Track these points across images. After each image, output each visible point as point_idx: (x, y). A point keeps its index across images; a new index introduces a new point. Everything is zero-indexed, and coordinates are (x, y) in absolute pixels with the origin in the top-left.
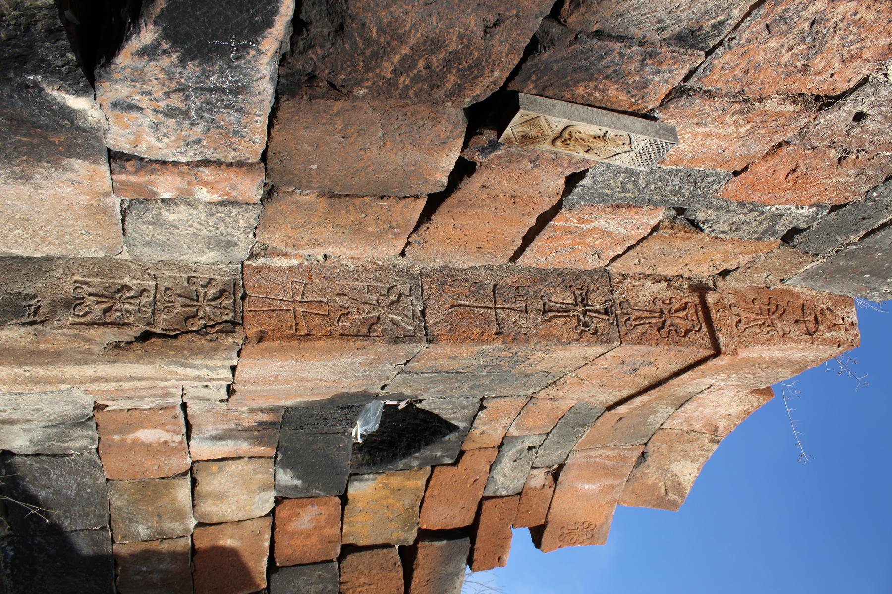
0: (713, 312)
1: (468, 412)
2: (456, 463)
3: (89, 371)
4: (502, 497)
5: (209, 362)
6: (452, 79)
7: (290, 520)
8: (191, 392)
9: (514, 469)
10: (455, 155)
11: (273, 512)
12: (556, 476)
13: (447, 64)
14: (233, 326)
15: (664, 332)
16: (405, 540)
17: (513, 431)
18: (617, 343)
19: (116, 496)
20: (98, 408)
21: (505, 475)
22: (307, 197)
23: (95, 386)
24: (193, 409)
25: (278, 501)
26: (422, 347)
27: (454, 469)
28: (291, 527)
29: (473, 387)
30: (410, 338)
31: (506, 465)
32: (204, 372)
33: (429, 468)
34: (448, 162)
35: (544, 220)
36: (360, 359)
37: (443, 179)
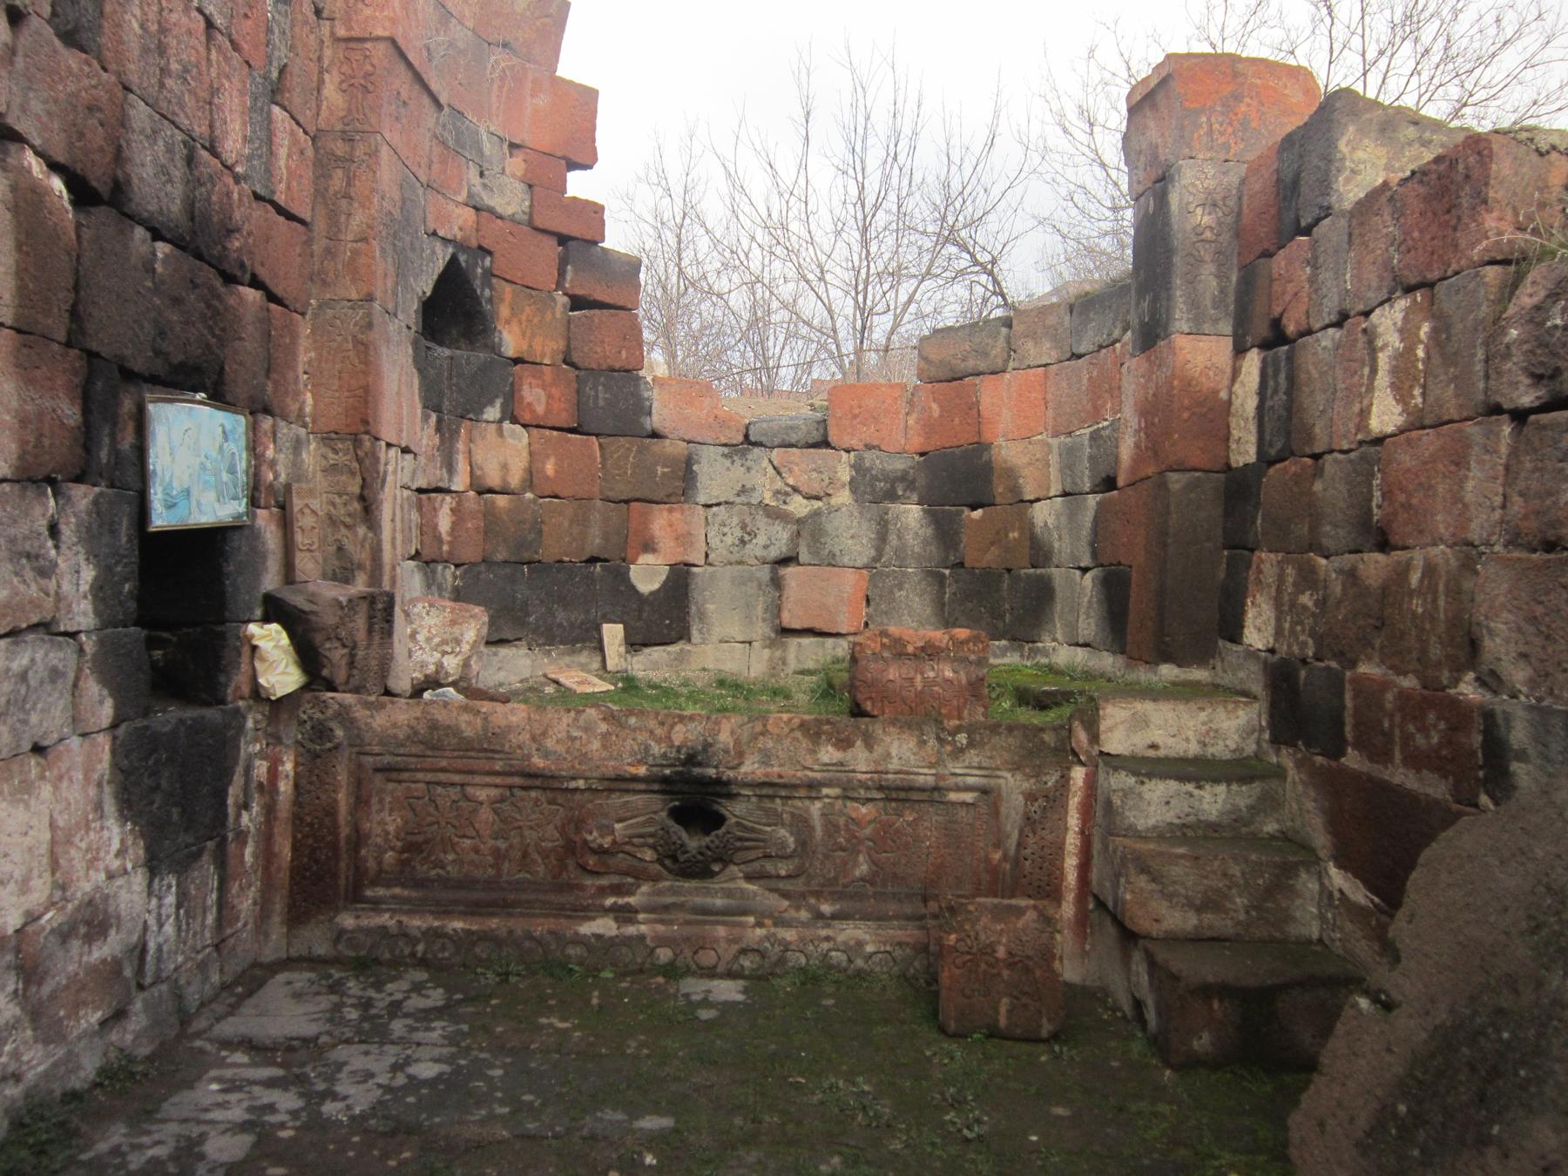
0: (353, 34)
1: (438, 246)
2: (490, 253)
4: (531, 206)
5: (382, 461)
6: (215, 303)
7: (533, 411)
8: (406, 480)
9: (502, 193)
11: (525, 426)
12: (513, 146)
13: (209, 306)
14: (357, 442)
15: (371, 88)
16: (564, 306)
17: (461, 198)
18: (379, 137)
20: (416, 556)
21: (508, 204)
22: (270, 387)
23: (399, 551)
24: (422, 483)
25: (514, 421)
26: (376, 305)
27: (497, 255)
28: (540, 409)
29: (413, 249)
30: (369, 315)
32: (390, 468)
33: (494, 280)
34: (251, 295)
35: (281, 211)
36: (384, 350)
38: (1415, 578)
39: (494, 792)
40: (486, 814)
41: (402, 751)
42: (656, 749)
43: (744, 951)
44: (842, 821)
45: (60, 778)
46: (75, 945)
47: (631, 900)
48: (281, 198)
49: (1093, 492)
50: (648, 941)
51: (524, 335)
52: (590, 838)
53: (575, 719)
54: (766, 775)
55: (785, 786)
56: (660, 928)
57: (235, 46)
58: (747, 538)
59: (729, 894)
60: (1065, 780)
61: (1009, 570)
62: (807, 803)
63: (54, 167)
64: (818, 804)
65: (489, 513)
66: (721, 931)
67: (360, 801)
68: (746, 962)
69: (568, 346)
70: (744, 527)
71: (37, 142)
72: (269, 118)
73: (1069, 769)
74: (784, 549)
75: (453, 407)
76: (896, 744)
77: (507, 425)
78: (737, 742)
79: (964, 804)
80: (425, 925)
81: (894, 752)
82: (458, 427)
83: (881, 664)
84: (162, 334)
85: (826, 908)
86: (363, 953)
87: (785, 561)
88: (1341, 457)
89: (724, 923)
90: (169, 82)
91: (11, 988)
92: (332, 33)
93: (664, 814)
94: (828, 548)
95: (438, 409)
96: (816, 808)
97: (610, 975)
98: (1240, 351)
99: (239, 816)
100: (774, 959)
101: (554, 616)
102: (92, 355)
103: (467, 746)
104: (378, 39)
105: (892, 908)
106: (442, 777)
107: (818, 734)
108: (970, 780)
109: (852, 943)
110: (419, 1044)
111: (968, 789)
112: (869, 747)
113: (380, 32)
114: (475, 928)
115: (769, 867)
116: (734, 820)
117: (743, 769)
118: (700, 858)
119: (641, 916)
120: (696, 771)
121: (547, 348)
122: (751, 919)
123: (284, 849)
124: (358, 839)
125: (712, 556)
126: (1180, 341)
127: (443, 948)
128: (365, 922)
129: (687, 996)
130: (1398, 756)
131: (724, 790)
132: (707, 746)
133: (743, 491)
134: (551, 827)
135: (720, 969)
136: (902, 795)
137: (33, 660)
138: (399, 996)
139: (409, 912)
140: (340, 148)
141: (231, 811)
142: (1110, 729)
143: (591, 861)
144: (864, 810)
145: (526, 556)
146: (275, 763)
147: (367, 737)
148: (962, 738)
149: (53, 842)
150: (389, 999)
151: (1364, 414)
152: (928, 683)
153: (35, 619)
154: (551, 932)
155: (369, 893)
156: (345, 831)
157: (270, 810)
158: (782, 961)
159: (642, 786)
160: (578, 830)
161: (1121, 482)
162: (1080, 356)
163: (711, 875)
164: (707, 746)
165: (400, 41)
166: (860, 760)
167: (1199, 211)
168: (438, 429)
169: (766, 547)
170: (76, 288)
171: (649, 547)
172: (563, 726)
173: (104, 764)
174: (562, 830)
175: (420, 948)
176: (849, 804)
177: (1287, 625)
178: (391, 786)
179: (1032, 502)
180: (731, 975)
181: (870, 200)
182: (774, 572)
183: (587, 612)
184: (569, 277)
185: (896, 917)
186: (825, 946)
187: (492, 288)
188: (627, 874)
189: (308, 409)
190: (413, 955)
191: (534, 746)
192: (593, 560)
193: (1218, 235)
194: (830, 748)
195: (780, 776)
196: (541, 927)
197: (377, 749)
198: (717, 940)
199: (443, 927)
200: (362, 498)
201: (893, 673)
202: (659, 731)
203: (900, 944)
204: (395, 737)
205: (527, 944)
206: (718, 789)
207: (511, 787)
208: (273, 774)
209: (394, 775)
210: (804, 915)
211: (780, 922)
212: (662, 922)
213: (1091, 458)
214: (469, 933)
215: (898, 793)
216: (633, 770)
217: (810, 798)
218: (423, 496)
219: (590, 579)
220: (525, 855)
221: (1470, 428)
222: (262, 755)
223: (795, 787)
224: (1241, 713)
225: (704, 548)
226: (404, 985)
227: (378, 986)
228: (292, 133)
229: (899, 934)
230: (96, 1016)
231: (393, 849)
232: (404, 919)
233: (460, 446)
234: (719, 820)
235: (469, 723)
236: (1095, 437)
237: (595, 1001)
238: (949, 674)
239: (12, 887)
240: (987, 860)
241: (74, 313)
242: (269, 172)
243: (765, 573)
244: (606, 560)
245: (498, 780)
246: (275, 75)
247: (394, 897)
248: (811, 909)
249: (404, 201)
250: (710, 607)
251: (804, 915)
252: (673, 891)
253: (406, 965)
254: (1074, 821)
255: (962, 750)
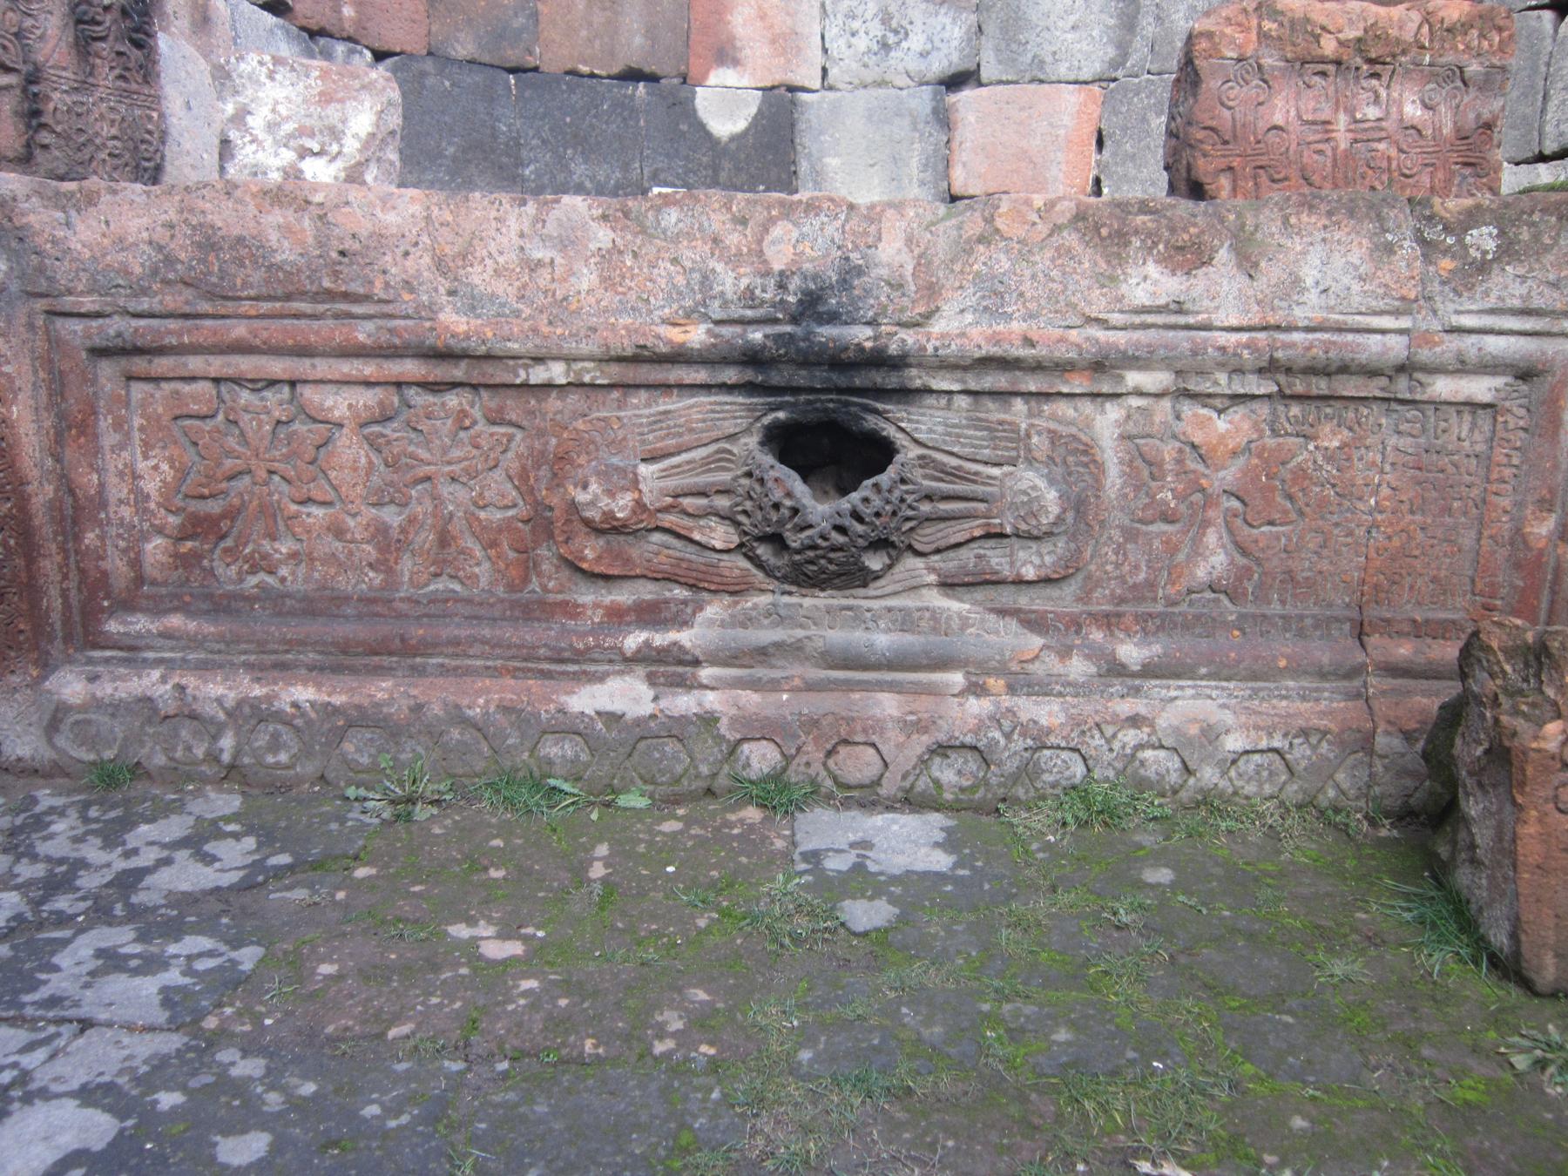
19: (459, 48)
40: (350, 449)
41: (145, 304)
42: (729, 281)
43: (942, 750)
44: (1168, 451)
47: (685, 637)
50: (723, 727)
52: (582, 497)
53: (539, 220)
54: (996, 339)
55: (1037, 367)
56: (751, 699)
58: (892, 39)
59: (906, 622)
62: (1087, 407)
64: (1114, 412)
66: (888, 705)
67: (73, 427)
68: (948, 774)
70: (886, 19)
74: (955, 58)
76: (1315, 258)
78: (923, 263)
80: (231, 697)
81: (1309, 275)
83: (1254, 88)
85: (1131, 652)
86: (109, 754)
87: (956, 81)
89: (892, 687)
93: (753, 441)
94: (1032, 49)
96: (1107, 423)
97: (642, 803)
100: (1011, 766)
101: (565, 168)
103: (287, 290)
105: (1283, 649)
106: (245, 365)
107: (1121, 237)
108: (1495, 345)
109: (1194, 730)
110: (86, 1025)
111: (1488, 367)
112: (1248, 264)
114: (339, 700)
115: (997, 559)
116: (915, 452)
117: (938, 327)
118: (839, 539)
119: (706, 673)
120: (826, 332)
122: (957, 678)
124: (77, 511)
125: (834, 72)
127: (275, 745)
128: (105, 689)
129: (814, 857)
131: (892, 381)
132: (850, 273)
134: (498, 474)
135: (888, 789)
136: (1321, 386)
138: (148, 857)
139: (203, 667)
143: (590, 550)
144: (1222, 425)
145: (513, 56)
147: (63, 273)
148: (1483, 239)
150: (121, 865)
152: (1364, 134)
154: (505, 709)
155: (113, 627)
156: (42, 493)
158: (1028, 771)
159: (701, 375)
160: (557, 480)
163: (864, 578)
164: (850, 273)
166: (1224, 297)
169: (924, 55)
171: (726, 55)
172: (510, 236)
174: (522, 479)
175: (227, 743)
176: (1188, 409)
178: (138, 390)
180: (911, 802)
182: (936, 97)
183: (626, 167)
185: (1295, 671)
186: (1130, 737)
188: (670, 579)
190: (213, 757)
191: (444, 285)
192: (633, 75)
194: (1152, 269)
195: (1029, 342)
196: (483, 698)
197: (89, 303)
198: (878, 726)
199: (269, 698)
201: (1282, 109)
202: (733, 239)
203: (1304, 733)
204: (125, 271)
205: (455, 734)
206: (878, 378)
207: (399, 385)
209: (139, 364)
210: (1078, 668)
211: (1022, 683)
212: (754, 685)
214: (329, 711)
215: (1309, 380)
216: (675, 335)
217: (1095, 396)
219: (626, 109)
220: (444, 540)
223: (1064, 368)
225: (818, 59)
226: (174, 827)
227: (112, 836)
229: (1305, 711)
231: (160, 531)
232: (190, 681)
234: (879, 452)
235: (286, 230)
237: (598, 871)
238: (1413, 111)
240: (1519, 537)
243: (922, 101)
244: (653, 78)
245: (369, 369)
247: (166, 635)
248: (1093, 654)
250: (832, 162)
251: (1078, 668)
252: (777, 617)
253: (204, 780)
255: (1483, 267)
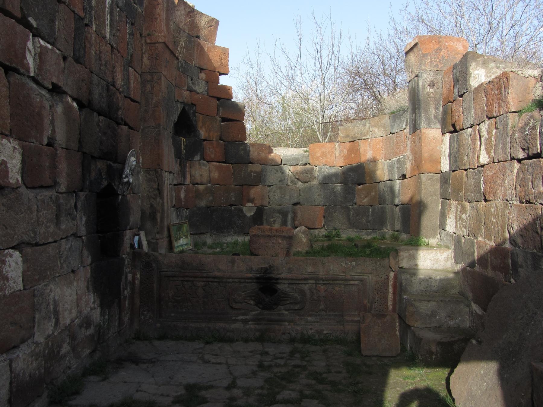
1: (179, 105)
2: (195, 105)
3: (166, 204)
9: (198, 85)
10: (124, 126)
11: (208, 162)
12: (201, 70)
14: (156, 172)
17: (186, 88)
20: (174, 206)
24: (175, 182)
25: (204, 160)
26: (161, 127)
28: (213, 156)
31: (197, 88)
33: (196, 114)
35: (132, 100)
37: (127, 127)
38: (493, 210)
39: (203, 283)
45: (78, 280)
46: (83, 329)
48: (132, 96)
49: (398, 179)
51: (206, 131)
56: (257, 326)
57: (119, 52)
60: (388, 276)
61: (372, 206)
63: (74, 99)
64: (307, 285)
65: (197, 191)
69: (221, 134)
71: (70, 93)
72: (128, 72)
73: (389, 273)
75: (184, 158)
77: (202, 162)
79: (354, 285)
82: (186, 163)
84: (101, 144)
88: (472, 170)
90: (102, 68)
91: (68, 342)
92: (145, 41)
95: (180, 158)
98: (443, 134)
99: (124, 291)
102: (84, 153)
104: (161, 43)
106: (186, 279)
113: (161, 41)
119: (250, 323)
121: (214, 136)
123: (137, 302)
125: (271, 203)
126: (424, 130)
130: (490, 267)
133: (281, 181)
137: (71, 245)
140: (149, 78)
141: (122, 289)
142: (402, 260)
146: (134, 275)
149: (77, 299)
151: (478, 157)
153: (71, 233)
157: (133, 289)
161: (407, 177)
162: (393, 134)
165: (167, 43)
167: (428, 87)
168: (180, 165)
170: (80, 134)
173: (89, 275)
177: (458, 225)
179: (379, 183)
181: (324, 68)
184: (221, 111)
187: (196, 117)
189: (141, 161)
193: (435, 95)
197: (166, 270)
200: (158, 189)
207: (208, 282)
208: (134, 278)
209: (171, 279)
212: (258, 324)
213: (397, 168)
218: (176, 187)
221: (506, 164)
222: (130, 272)
224: (445, 253)
228: (135, 75)
230: (88, 351)
233: (187, 169)
236: (399, 160)
239: (68, 312)
241: (80, 142)
242: (129, 88)
245: (204, 279)
246: (130, 58)
249: (168, 92)
254: (391, 290)
